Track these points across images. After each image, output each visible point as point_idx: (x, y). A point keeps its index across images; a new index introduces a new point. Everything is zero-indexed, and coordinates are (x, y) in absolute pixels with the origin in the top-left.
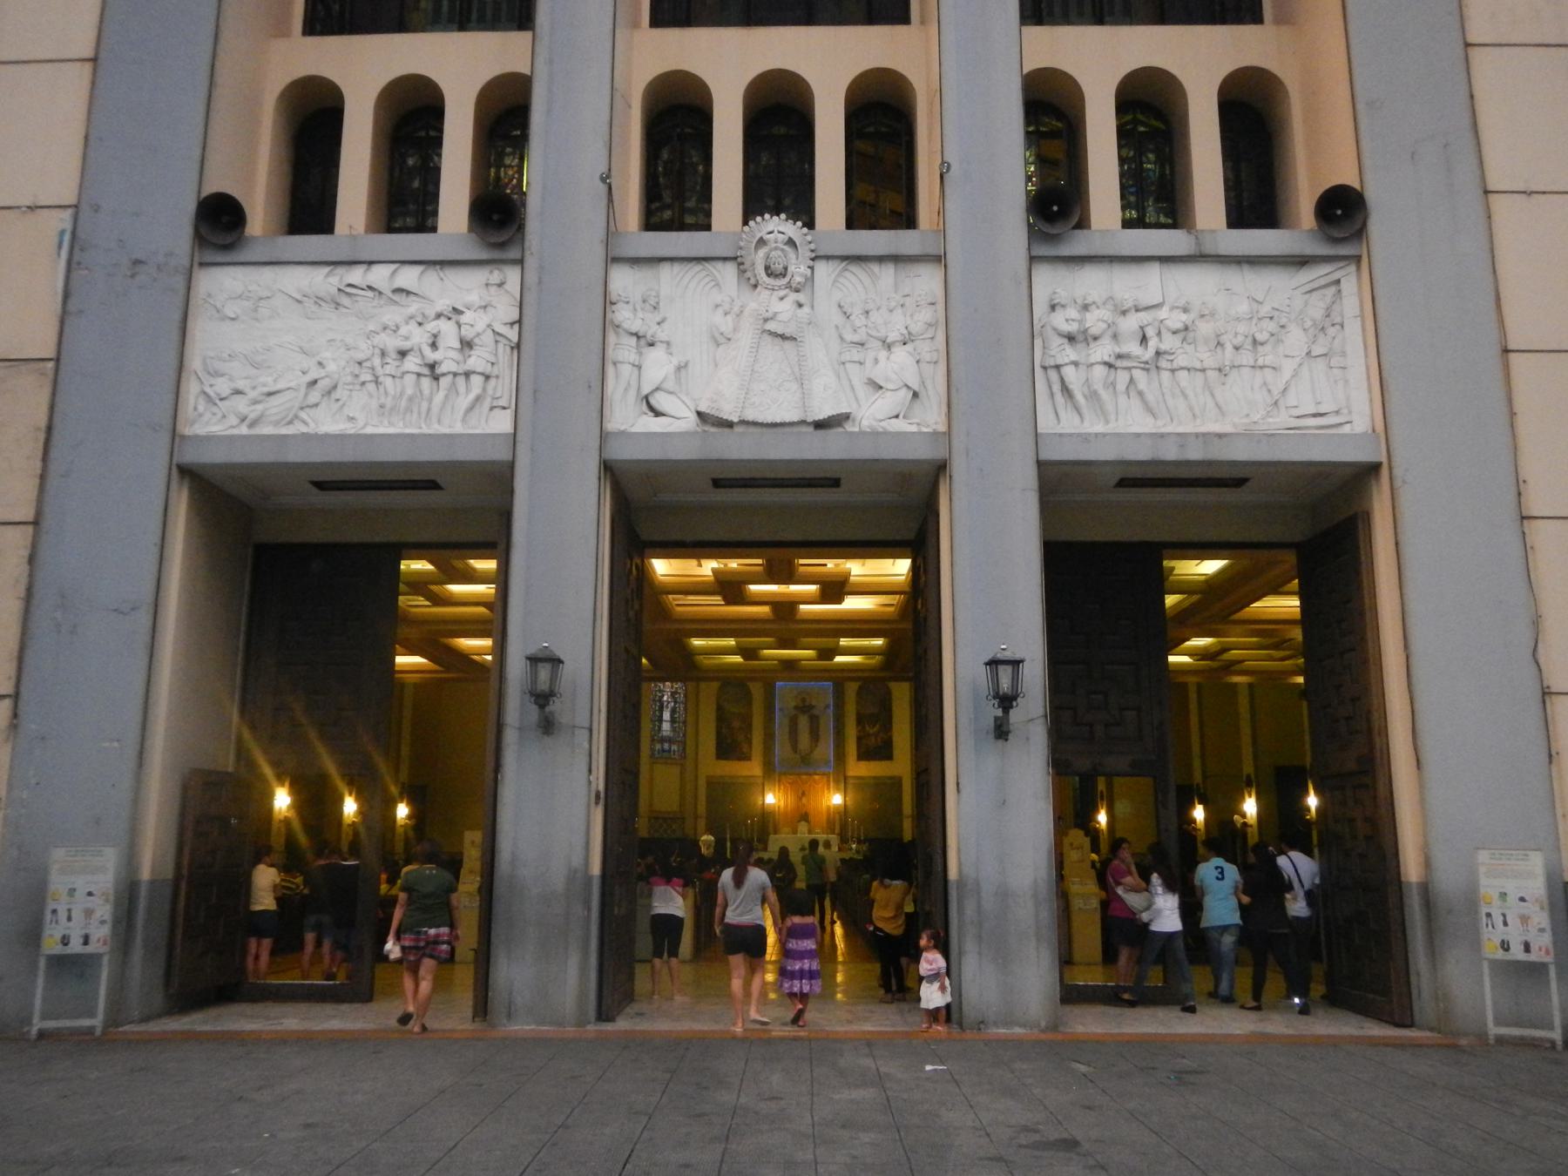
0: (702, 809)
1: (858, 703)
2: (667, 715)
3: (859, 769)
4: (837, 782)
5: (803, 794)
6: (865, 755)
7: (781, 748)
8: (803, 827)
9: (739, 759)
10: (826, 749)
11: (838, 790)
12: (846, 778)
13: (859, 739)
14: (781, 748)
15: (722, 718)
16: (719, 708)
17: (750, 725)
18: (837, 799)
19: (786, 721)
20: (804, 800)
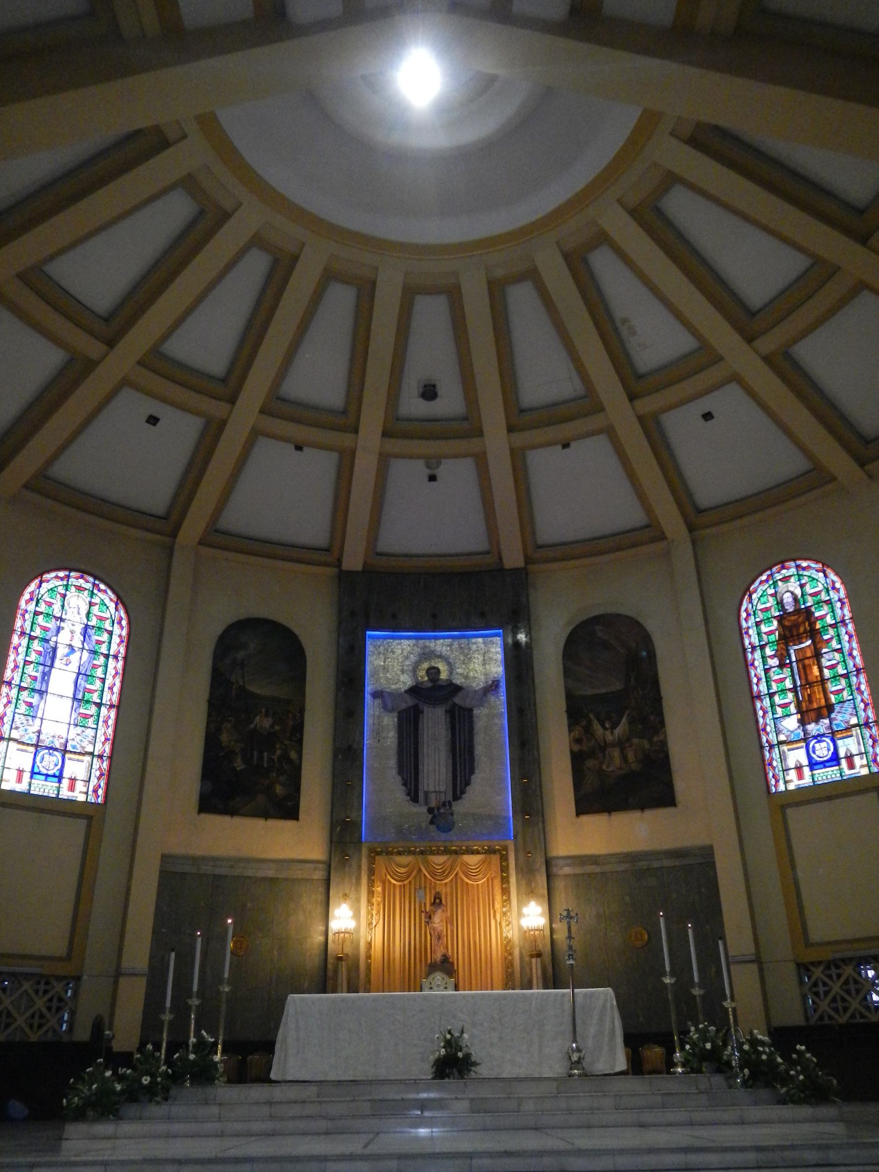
0: (138, 953)
1: (567, 672)
2: (62, 680)
3: (580, 836)
4: (526, 872)
5: (437, 902)
6: (592, 800)
7: (380, 787)
8: (438, 989)
9: (266, 816)
10: (494, 786)
11: (530, 893)
12: (548, 863)
13: (577, 759)
14: (380, 787)
15: (226, 702)
16: (218, 679)
17: (299, 728)
18: (533, 916)
19: (390, 721)
20: (438, 920)
